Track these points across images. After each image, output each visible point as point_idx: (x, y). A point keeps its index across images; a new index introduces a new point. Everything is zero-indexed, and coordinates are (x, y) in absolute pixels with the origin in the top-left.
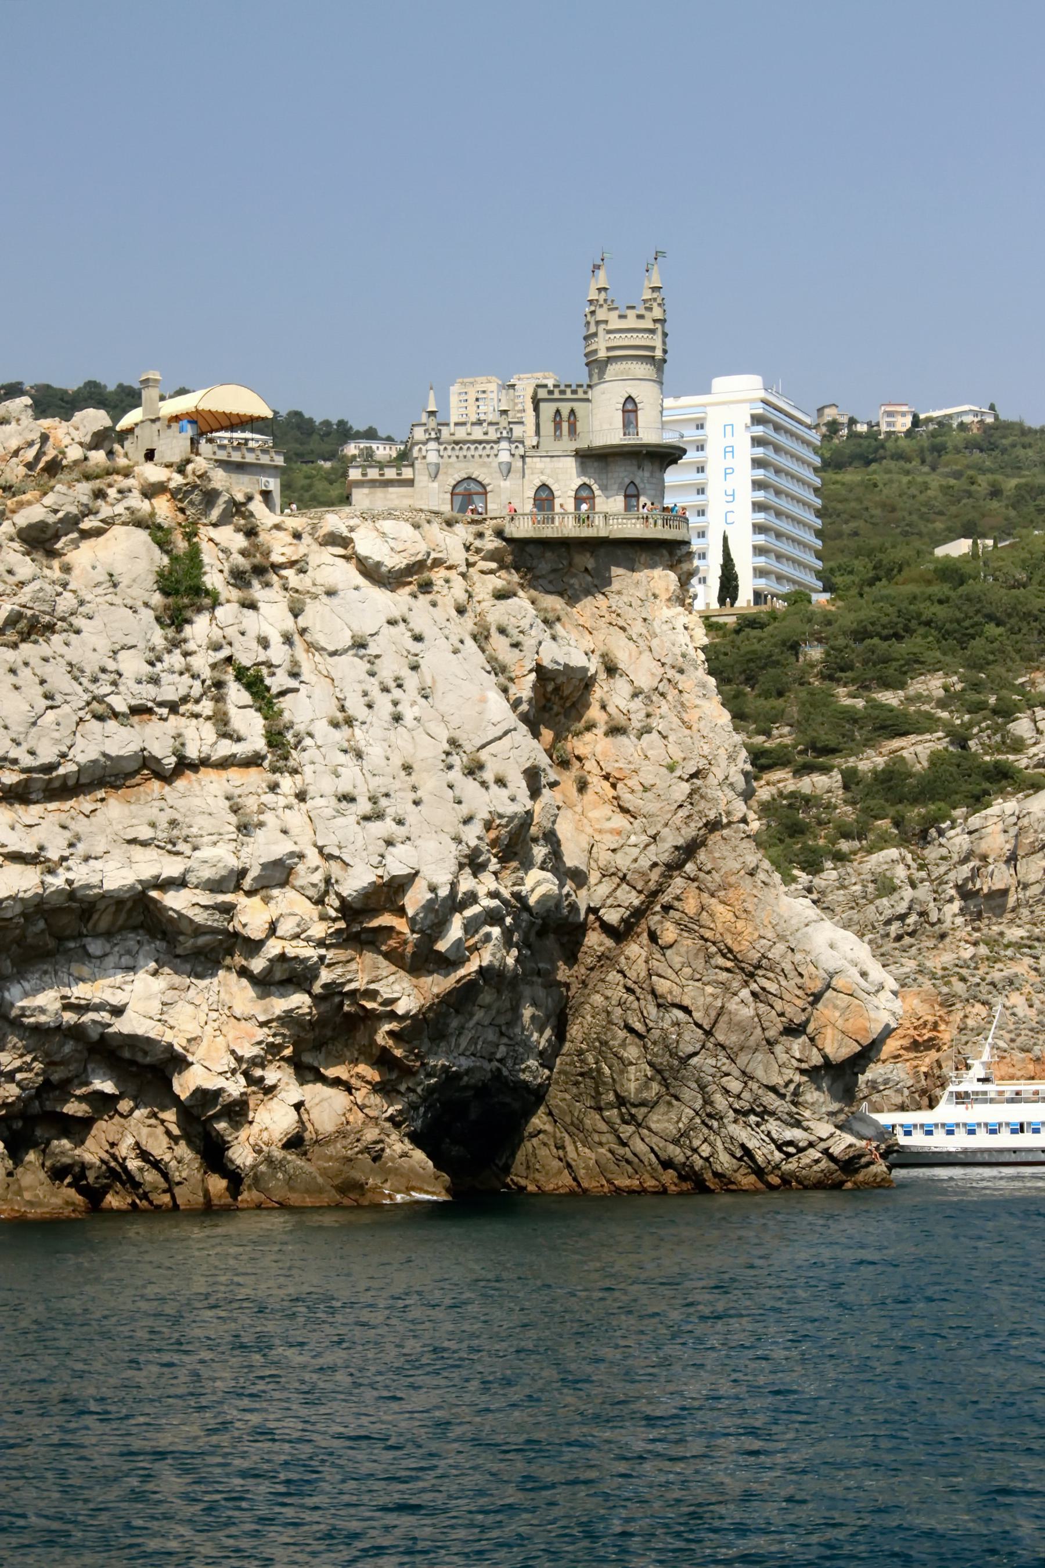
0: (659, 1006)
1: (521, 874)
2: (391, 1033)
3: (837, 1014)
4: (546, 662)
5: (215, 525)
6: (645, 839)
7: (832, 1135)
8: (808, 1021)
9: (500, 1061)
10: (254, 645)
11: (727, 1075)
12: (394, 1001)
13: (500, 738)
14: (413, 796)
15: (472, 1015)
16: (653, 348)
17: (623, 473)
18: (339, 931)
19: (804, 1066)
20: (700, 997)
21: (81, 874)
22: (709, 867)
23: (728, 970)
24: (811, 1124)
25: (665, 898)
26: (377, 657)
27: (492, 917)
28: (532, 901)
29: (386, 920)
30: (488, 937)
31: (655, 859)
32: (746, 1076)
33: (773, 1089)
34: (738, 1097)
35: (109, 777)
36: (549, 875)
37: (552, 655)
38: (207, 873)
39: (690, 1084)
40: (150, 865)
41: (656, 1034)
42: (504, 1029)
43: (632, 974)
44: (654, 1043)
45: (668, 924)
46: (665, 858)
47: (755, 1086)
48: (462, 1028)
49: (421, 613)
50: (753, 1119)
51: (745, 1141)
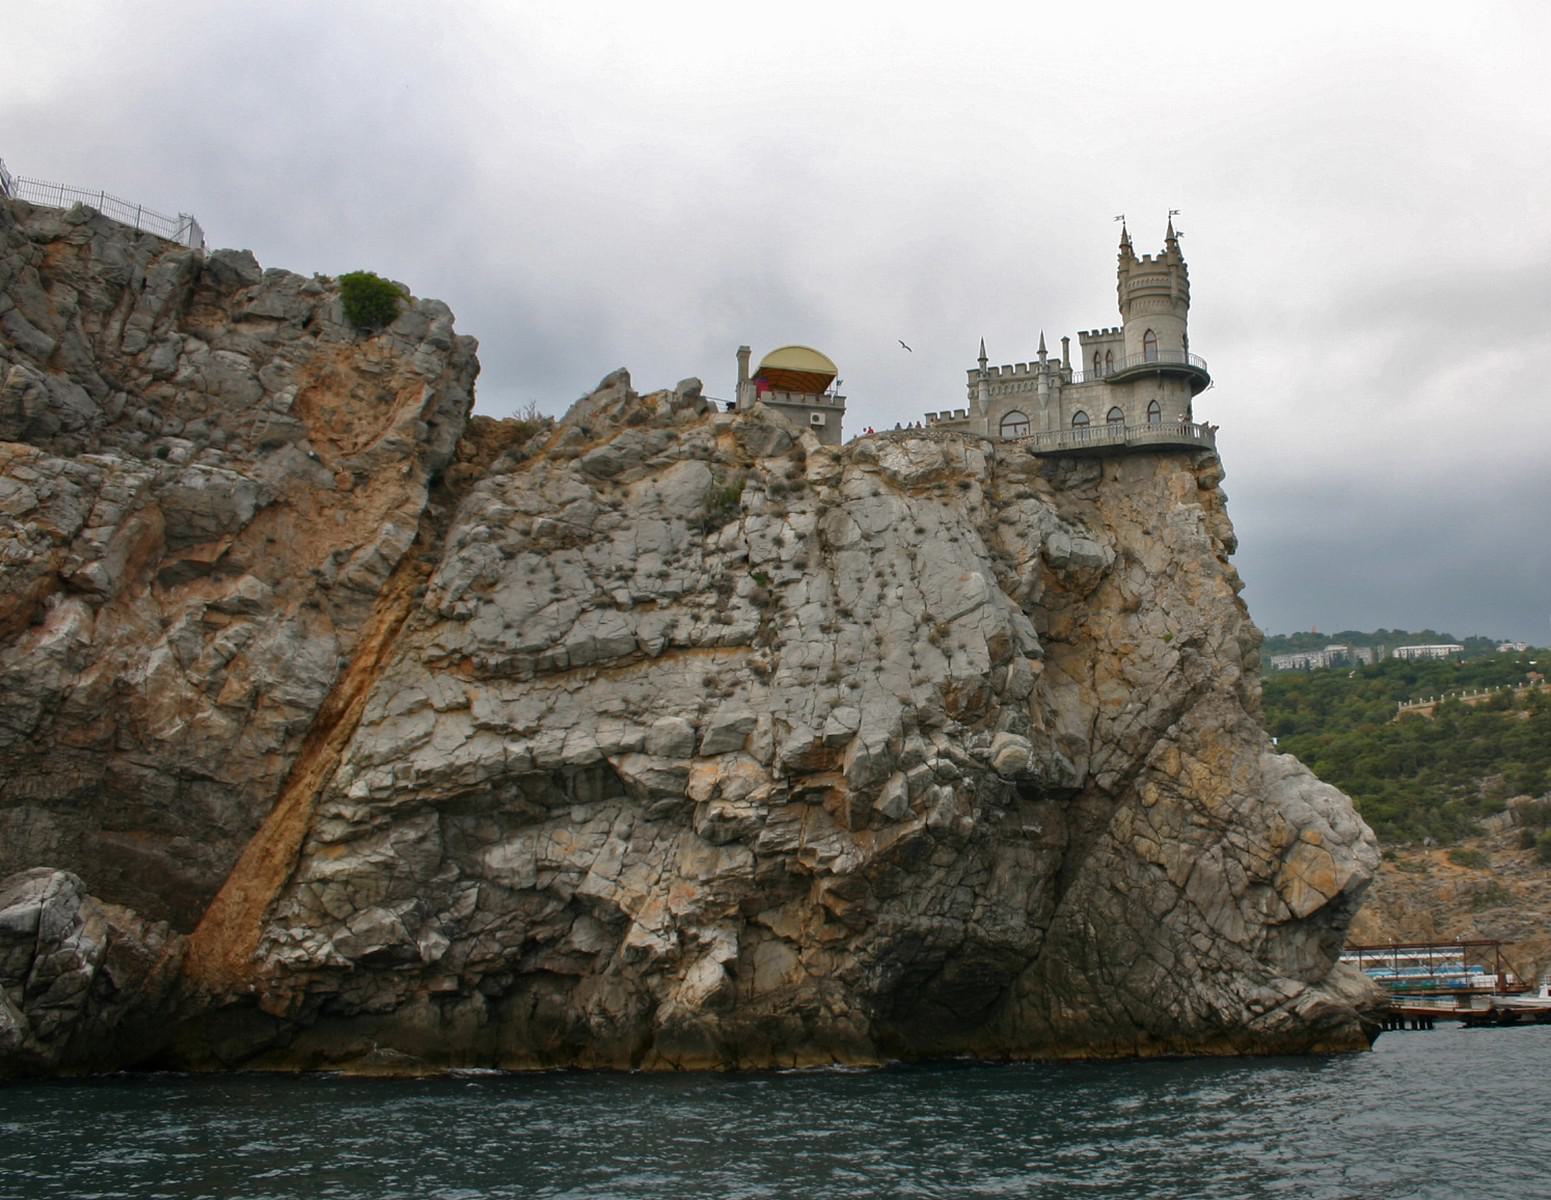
0: (1141, 864)
1: (987, 735)
2: (829, 891)
3: (1304, 866)
4: (1053, 551)
5: (771, 456)
6: (1139, 705)
7: (1299, 994)
8: (1274, 874)
9: (977, 921)
10: (770, 546)
11: (1198, 932)
12: (832, 859)
13: (972, 610)
14: (877, 663)
15: (929, 875)
17: (1145, 393)
18: (781, 792)
19: (1272, 921)
20: (1173, 854)
21: (542, 743)
22: (1189, 726)
23: (1201, 826)
24: (1279, 982)
25: (1149, 760)
26: (879, 550)
27: (942, 777)
28: (997, 763)
29: (826, 781)
31: (1143, 723)
32: (1215, 933)
33: (1239, 945)
34: (1206, 954)
35: (601, 661)
36: (1019, 738)
37: (1061, 544)
38: (663, 740)
39: (1163, 941)
40: (613, 734)
41: (1135, 893)
42: (977, 889)
43: (1119, 835)
44: (1134, 902)
45: (1151, 785)
46: (1152, 721)
47: (1221, 943)
49: (930, 512)
50: (1222, 976)
51: (1212, 1000)
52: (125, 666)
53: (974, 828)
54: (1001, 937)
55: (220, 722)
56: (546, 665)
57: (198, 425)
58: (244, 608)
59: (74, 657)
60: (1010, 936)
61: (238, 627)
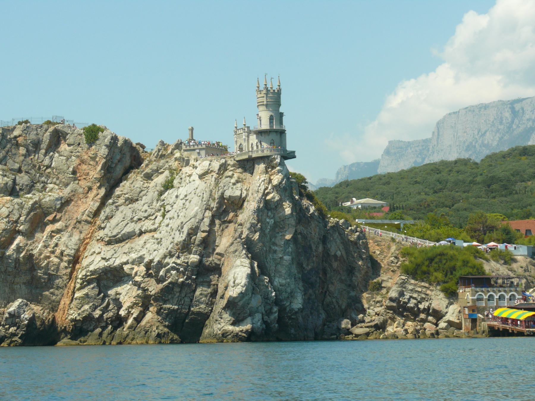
16: (263, 102)
27: (173, 268)
30: (171, 275)
36: (196, 256)
48: (173, 298)
52: (32, 250)
53: (183, 282)
54: (198, 310)
55: (56, 260)
56: (118, 240)
57: (55, 180)
58: (59, 231)
59: (19, 249)
60: (200, 310)
61: (58, 236)
